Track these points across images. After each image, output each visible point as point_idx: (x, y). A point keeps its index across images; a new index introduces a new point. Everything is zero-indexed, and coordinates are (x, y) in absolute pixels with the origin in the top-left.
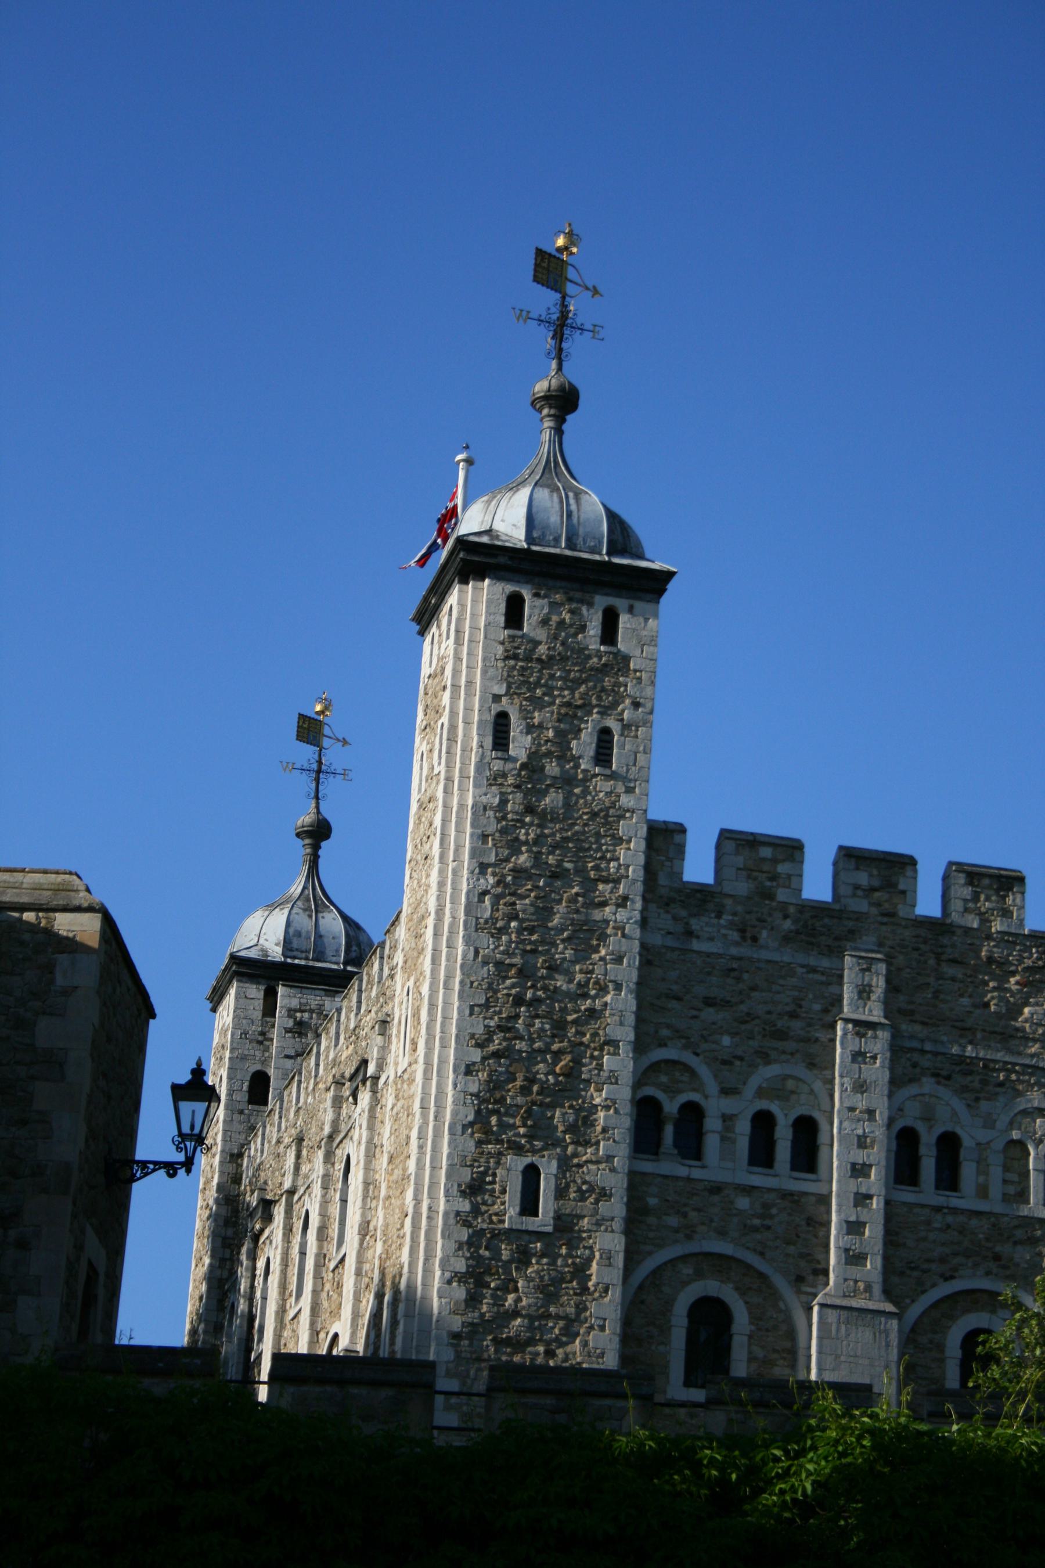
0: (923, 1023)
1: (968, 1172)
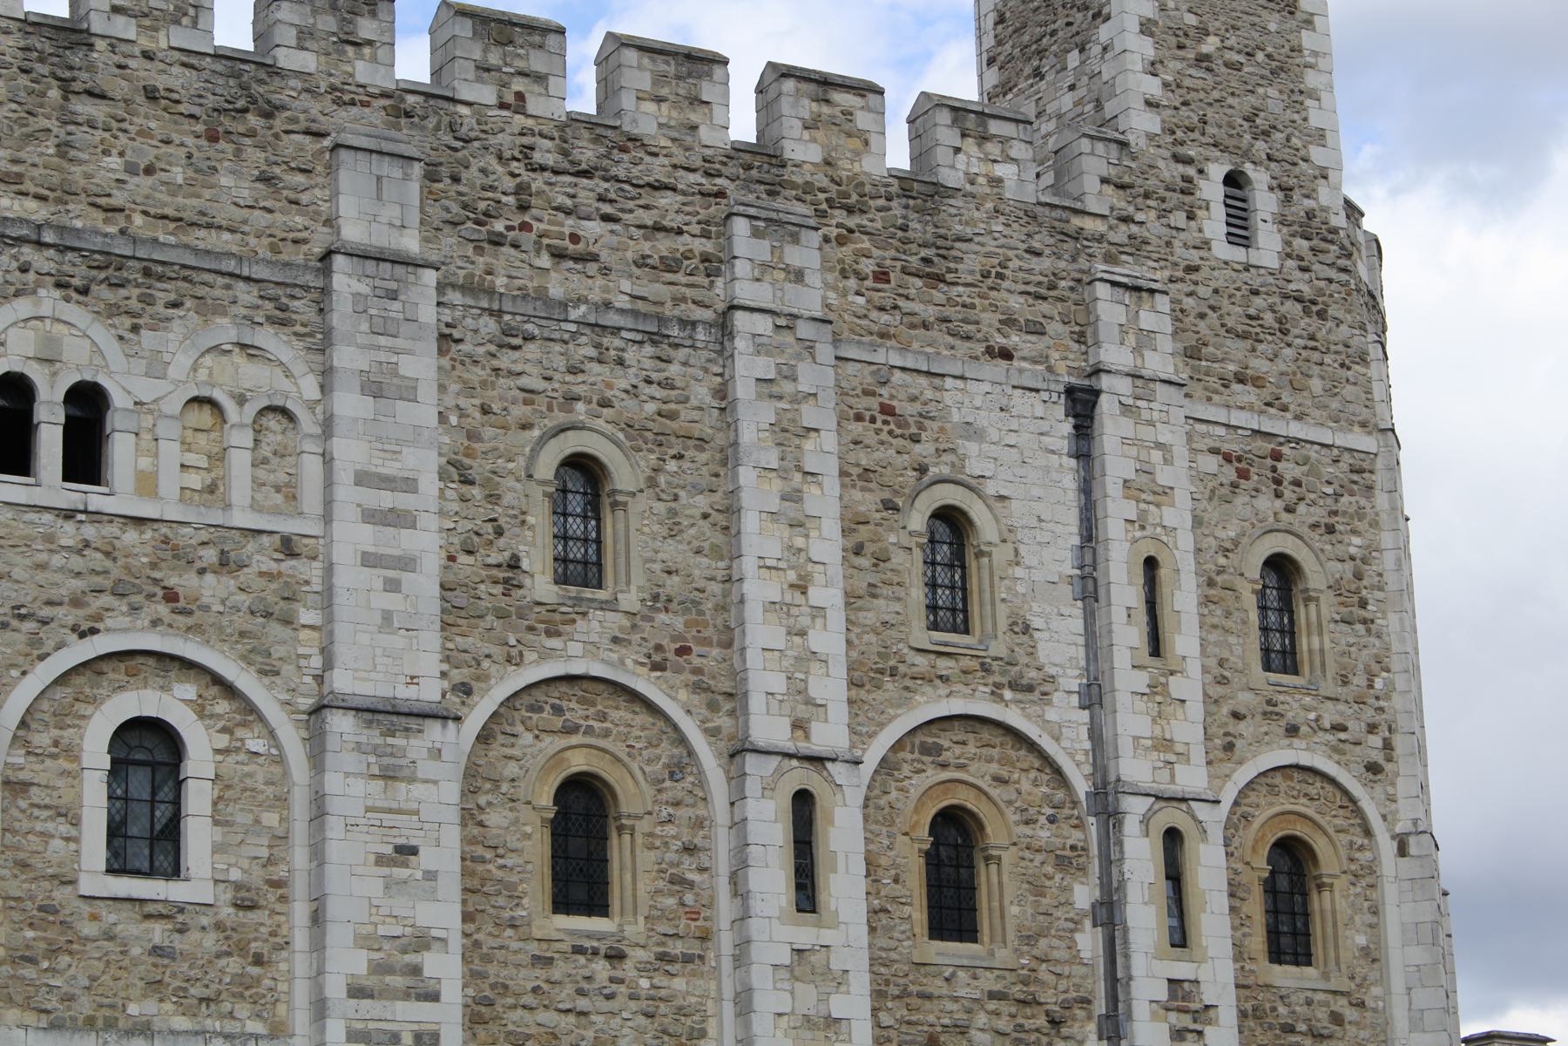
0: (38, 197)
1: (121, 452)
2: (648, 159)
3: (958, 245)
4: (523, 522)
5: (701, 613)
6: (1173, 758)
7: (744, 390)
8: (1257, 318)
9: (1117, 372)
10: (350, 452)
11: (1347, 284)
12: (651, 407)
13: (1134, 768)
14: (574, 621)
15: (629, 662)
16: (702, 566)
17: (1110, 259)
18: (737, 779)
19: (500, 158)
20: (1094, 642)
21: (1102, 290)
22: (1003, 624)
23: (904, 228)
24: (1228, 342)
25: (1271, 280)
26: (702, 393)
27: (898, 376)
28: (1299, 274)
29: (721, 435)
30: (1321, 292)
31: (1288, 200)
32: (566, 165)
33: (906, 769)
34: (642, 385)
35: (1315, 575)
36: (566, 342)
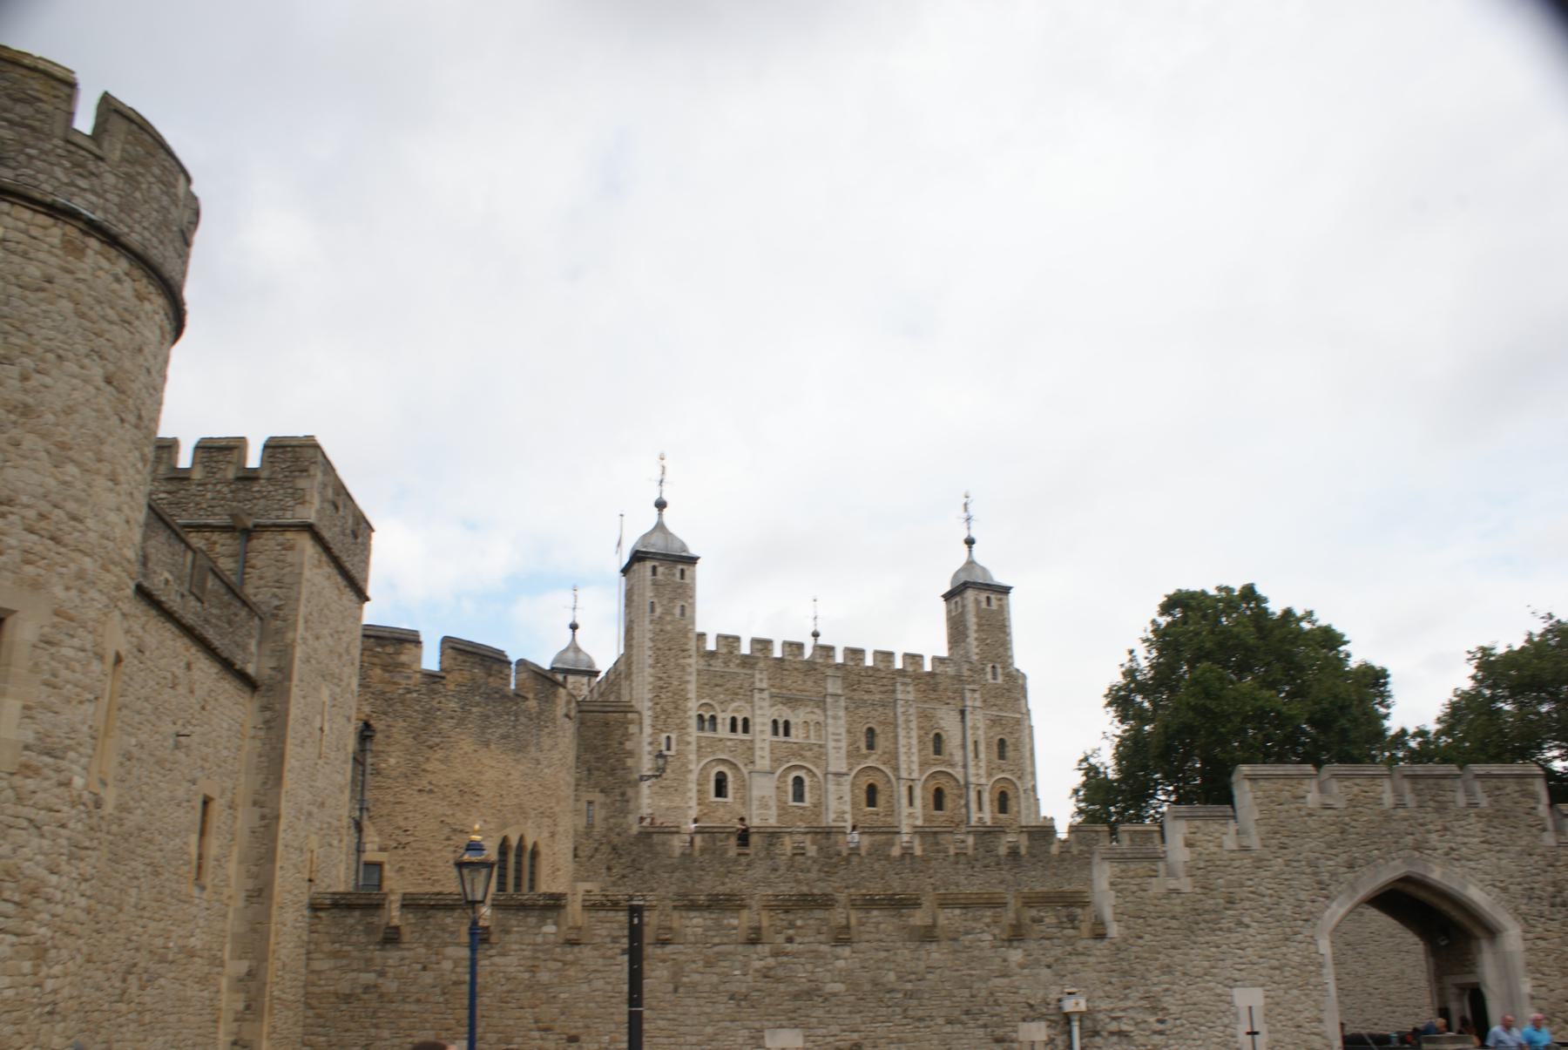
1: (793, 731)
10: (830, 729)
13: (972, 779)
20: (965, 756)
35: (1009, 741)
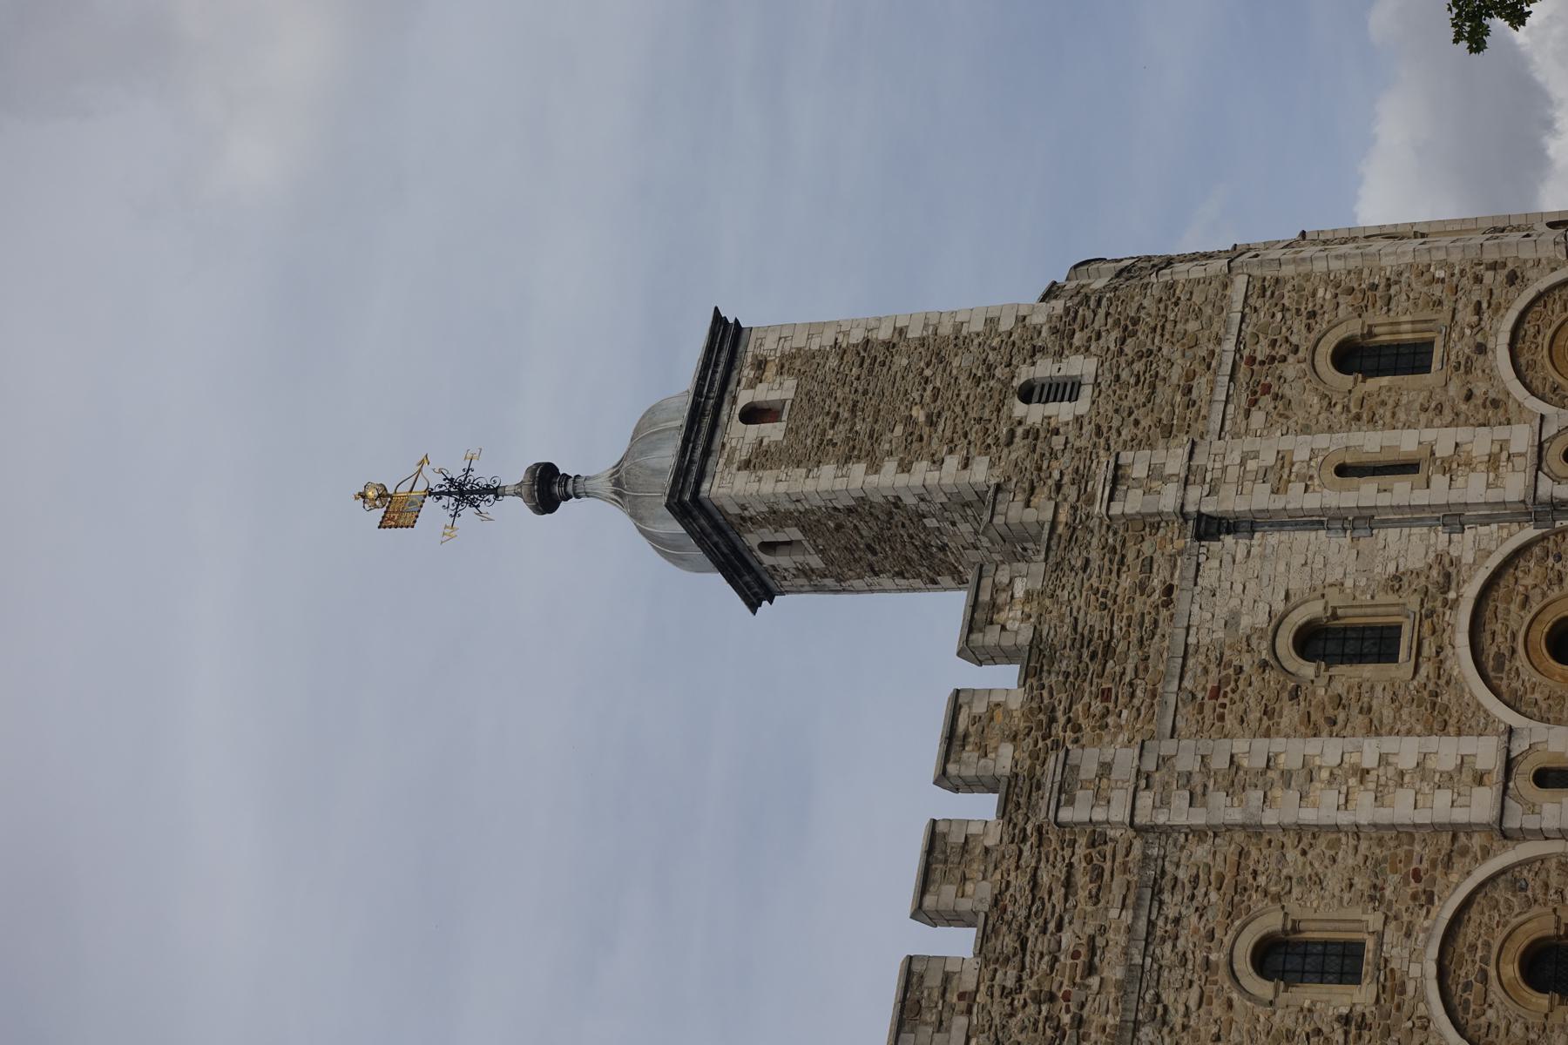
2: (1011, 890)
3: (1080, 629)
4: (1310, 1010)
5: (1385, 859)
6: (1504, 455)
7: (1199, 818)
8: (1138, 376)
9: (1183, 499)
11: (1110, 299)
12: (1213, 896)
13: (1514, 486)
14: (1392, 970)
15: (1426, 924)
16: (1347, 859)
17: (1090, 501)
18: (1523, 835)
19: (1011, 1015)
20: (1409, 517)
21: (1116, 509)
22: (1392, 598)
23: (1067, 675)
24: (1158, 401)
25: (1107, 364)
26: (1201, 852)
27: (1187, 684)
28: (1102, 341)
29: (1236, 836)
30: (1117, 323)
31: (1043, 350)
32: (1017, 959)
33: (1516, 684)
34: (1195, 903)
36: (1161, 967)
